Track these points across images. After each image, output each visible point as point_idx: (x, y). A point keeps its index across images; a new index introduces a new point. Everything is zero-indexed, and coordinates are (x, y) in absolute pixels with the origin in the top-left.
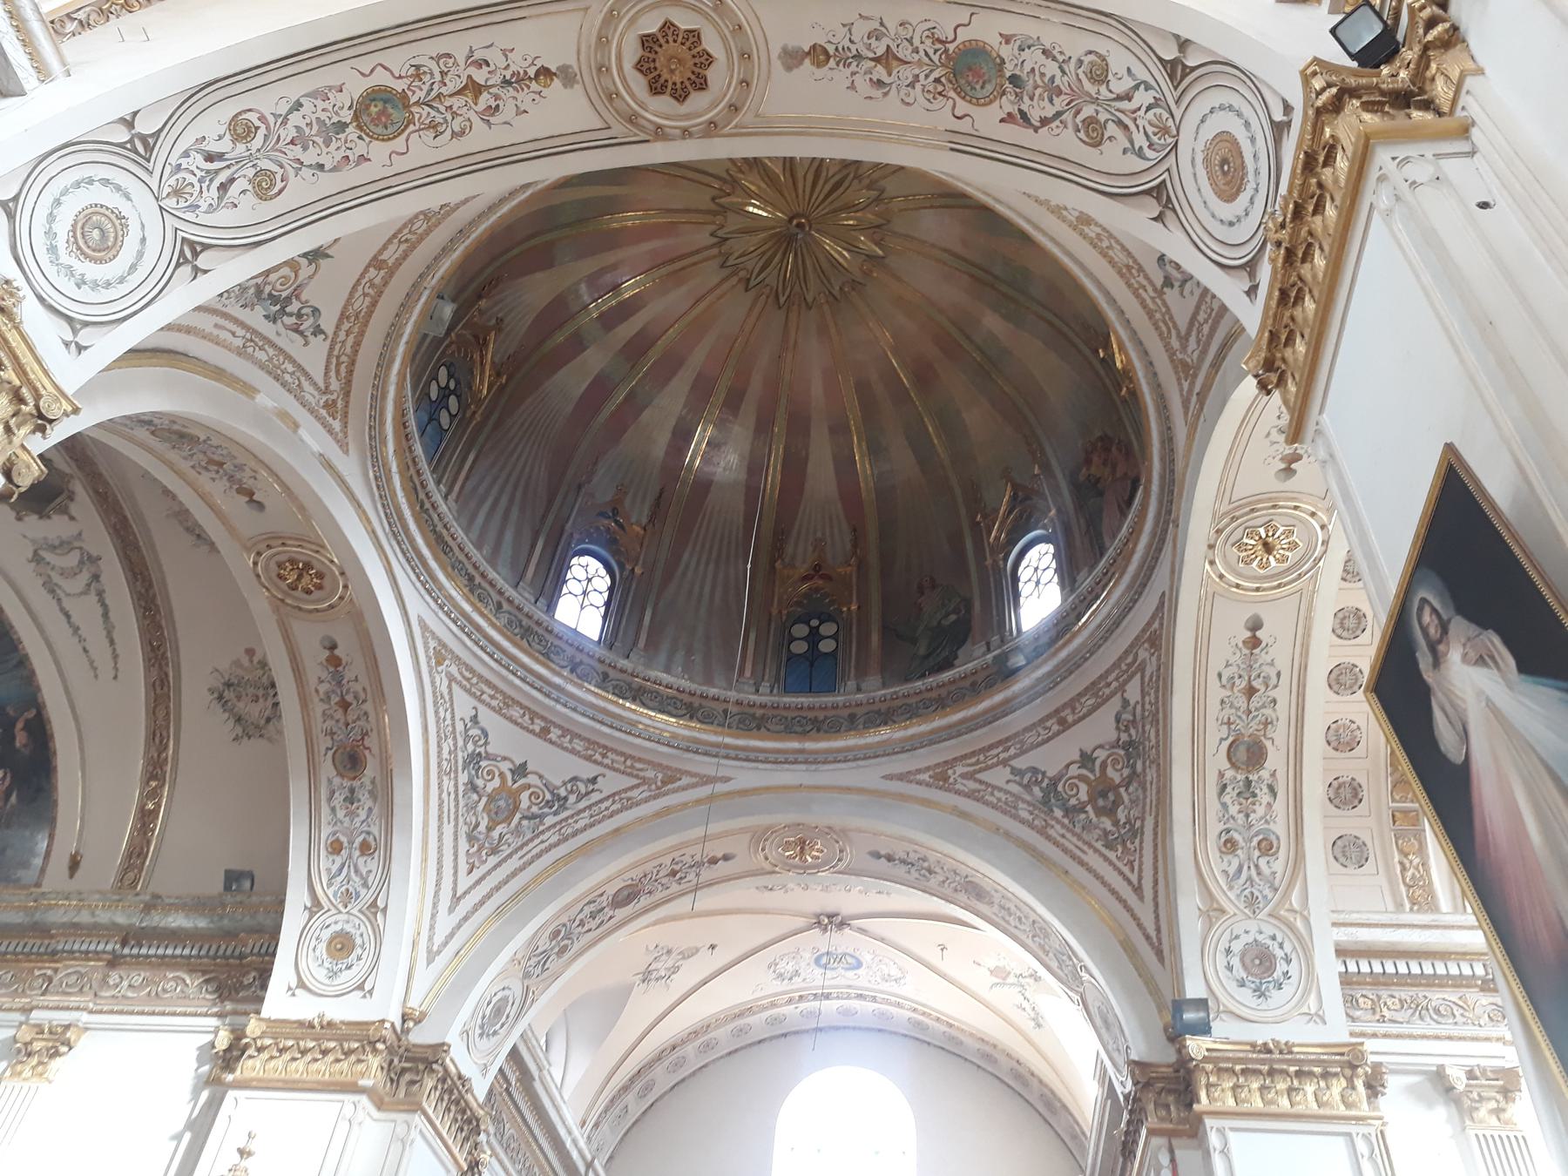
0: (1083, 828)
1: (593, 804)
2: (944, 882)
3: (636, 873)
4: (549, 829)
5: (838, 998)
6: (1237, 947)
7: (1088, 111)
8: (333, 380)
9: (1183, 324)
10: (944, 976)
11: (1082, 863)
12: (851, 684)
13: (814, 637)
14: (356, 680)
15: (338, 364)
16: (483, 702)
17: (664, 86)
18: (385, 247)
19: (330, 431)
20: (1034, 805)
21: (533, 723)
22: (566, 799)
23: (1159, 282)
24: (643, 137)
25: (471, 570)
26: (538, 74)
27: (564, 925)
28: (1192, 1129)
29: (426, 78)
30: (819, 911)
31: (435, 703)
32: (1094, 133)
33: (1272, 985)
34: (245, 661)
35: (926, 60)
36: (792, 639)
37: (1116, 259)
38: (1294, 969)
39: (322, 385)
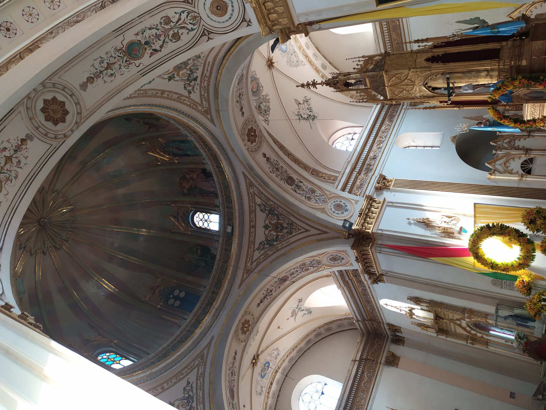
0: (283, 238)
1: (196, 387)
2: (275, 290)
4: (197, 406)
5: (273, 380)
6: (333, 210)
7: (171, 33)
9: (198, 100)
11: (292, 243)
12: (202, 289)
13: (176, 298)
17: (57, 121)
20: (270, 249)
21: (158, 390)
22: (189, 395)
24: (63, 141)
26: (21, 142)
32: (176, 37)
35: (119, 58)
37: (175, 98)
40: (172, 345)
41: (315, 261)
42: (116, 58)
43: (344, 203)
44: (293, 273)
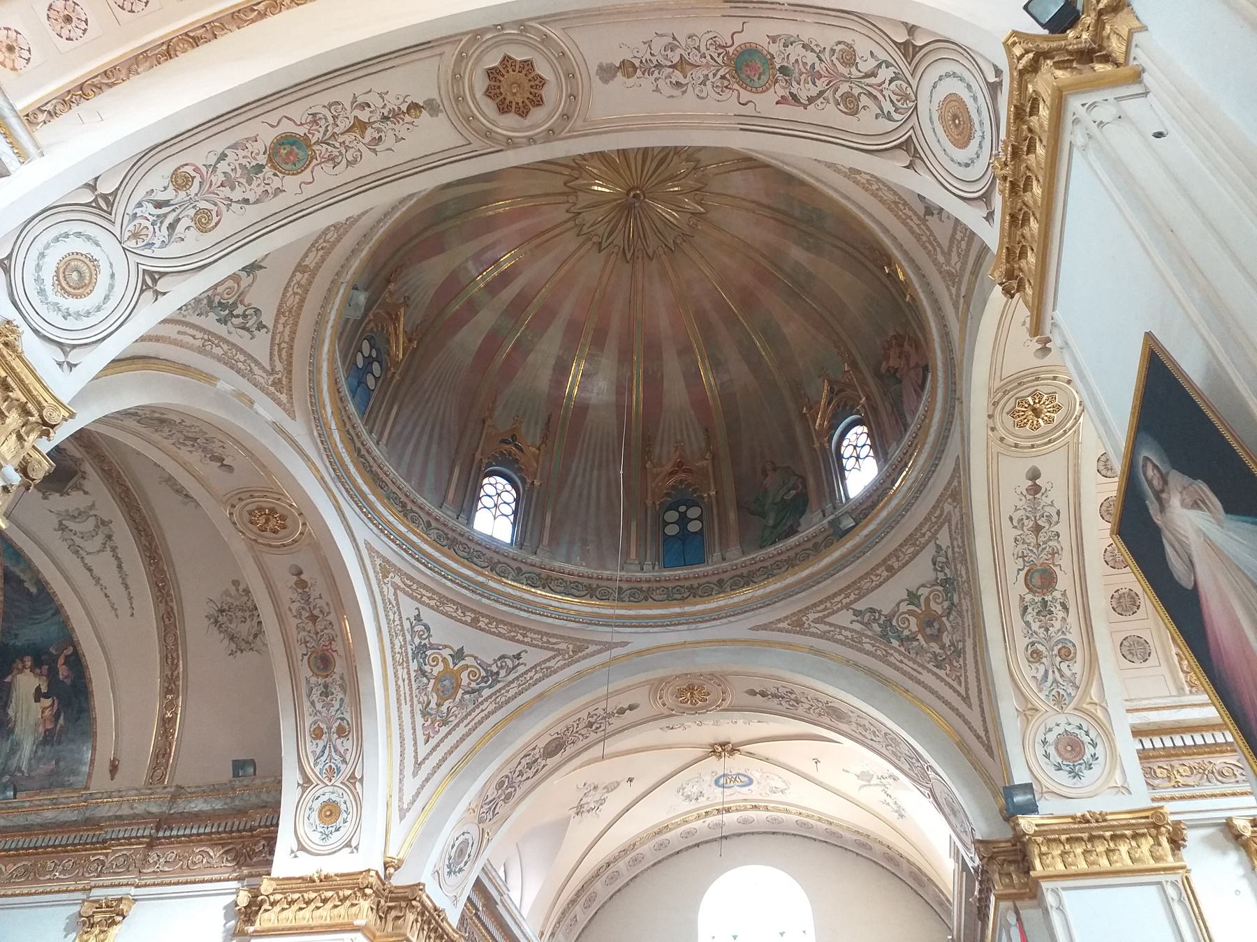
0: (917, 654)
2: (809, 709)
3: (560, 728)
4: (486, 700)
5: (737, 810)
6: (1051, 737)
7: (844, 88)
8: (277, 362)
9: (945, 243)
10: (819, 784)
11: (919, 682)
12: (717, 555)
13: (683, 520)
14: (321, 598)
15: (280, 350)
16: (423, 603)
17: (510, 105)
18: (306, 255)
19: (279, 404)
22: (498, 673)
23: (921, 212)
25: (403, 499)
26: (409, 109)
27: (507, 777)
28: (1031, 892)
29: (322, 122)
30: (713, 742)
31: (385, 609)
32: (850, 105)
34: (233, 592)
36: (666, 524)
38: (1099, 751)
39: (268, 368)
42: (705, 57)
43: (1093, 756)
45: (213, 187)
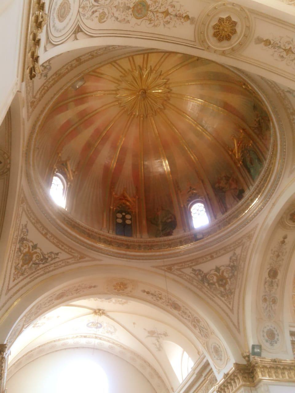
2: (164, 302)
4: (40, 269)
5: (89, 337)
6: (266, 330)
11: (213, 301)
12: (138, 235)
13: (124, 218)
15: (44, 89)
22: (47, 259)
26: (185, 17)
27: (41, 304)
29: (157, 4)
33: (274, 342)
36: (117, 218)
39: (34, 94)
40: (84, 229)
41: (207, 331)
43: (278, 339)
44: (185, 313)
45: (113, 6)
